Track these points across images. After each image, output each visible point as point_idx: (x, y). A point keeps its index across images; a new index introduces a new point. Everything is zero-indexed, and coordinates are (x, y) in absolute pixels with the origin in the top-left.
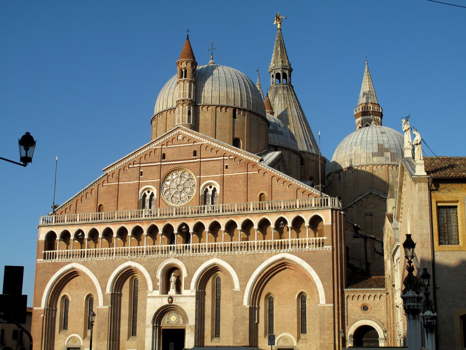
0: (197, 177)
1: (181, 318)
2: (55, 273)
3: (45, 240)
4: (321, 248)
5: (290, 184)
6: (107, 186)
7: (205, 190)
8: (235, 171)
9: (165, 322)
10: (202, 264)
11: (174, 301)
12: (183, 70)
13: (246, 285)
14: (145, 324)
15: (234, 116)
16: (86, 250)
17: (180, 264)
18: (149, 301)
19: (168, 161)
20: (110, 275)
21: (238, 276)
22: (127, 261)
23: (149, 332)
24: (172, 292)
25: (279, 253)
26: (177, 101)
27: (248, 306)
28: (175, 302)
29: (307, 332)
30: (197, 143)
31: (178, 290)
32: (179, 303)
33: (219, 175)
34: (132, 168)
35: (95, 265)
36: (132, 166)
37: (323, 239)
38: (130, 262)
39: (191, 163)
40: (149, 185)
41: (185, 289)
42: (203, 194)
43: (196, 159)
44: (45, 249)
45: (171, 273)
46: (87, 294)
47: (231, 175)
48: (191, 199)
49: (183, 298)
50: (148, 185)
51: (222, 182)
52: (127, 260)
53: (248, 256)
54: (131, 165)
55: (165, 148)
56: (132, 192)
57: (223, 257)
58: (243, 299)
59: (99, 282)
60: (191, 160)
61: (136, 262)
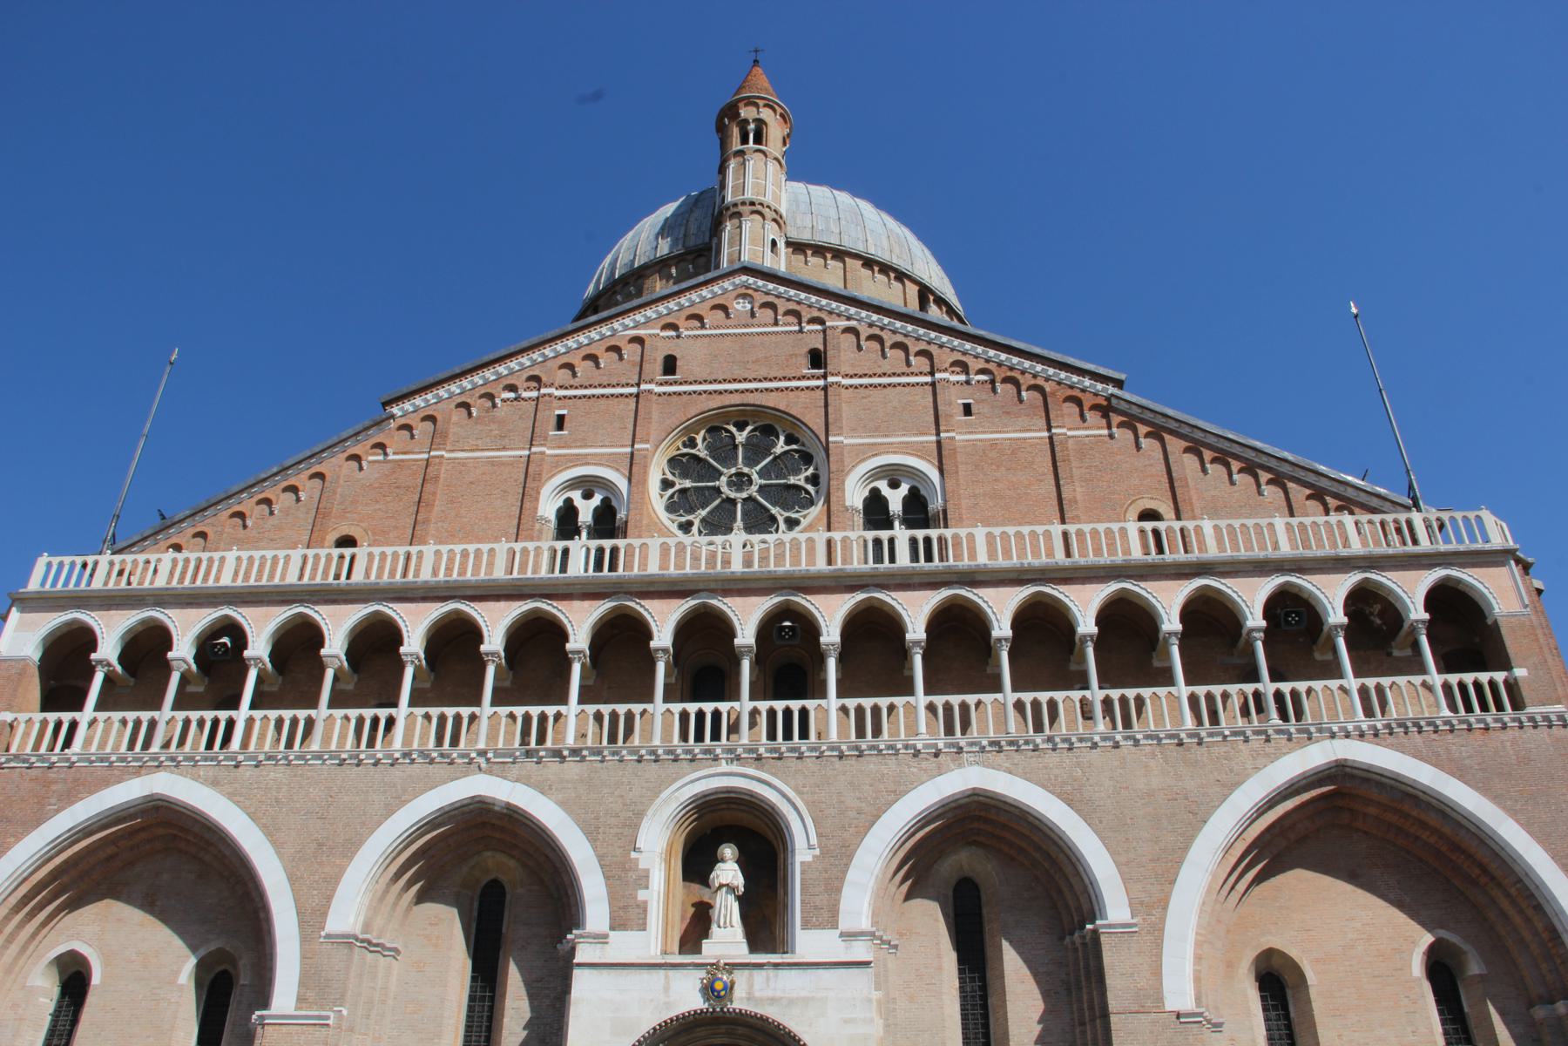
6: (389, 465)
7: (867, 494)
8: (1006, 425)
10: (898, 794)
11: (739, 992)
12: (752, 126)
13: (1164, 904)
18: (583, 985)
19: (691, 379)
20: (360, 843)
21: (1114, 854)
28: (748, 999)
30: (821, 322)
32: (773, 1000)
34: (515, 403)
35: (279, 790)
36: (512, 395)
37: (1512, 686)
39: (798, 393)
40: (595, 464)
42: (860, 506)
43: (825, 377)
46: (203, 952)
47: (994, 439)
49: (794, 973)
50: (587, 464)
53: (1154, 756)
54: (511, 391)
56: (505, 492)
57: (1017, 757)
58: (1157, 973)
60: (799, 379)
61: (517, 781)
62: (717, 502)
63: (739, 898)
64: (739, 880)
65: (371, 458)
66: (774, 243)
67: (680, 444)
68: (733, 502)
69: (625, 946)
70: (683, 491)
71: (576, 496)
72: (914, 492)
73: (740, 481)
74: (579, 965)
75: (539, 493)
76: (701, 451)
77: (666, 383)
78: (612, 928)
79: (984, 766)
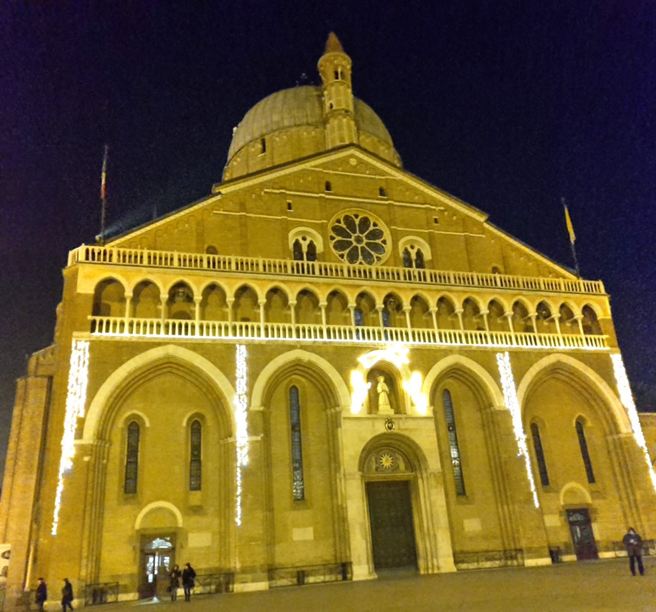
0: (392, 227)
9: (371, 466)
18: (346, 426)
28: (399, 429)
29: (596, 480)
30: (384, 176)
32: (406, 429)
38: (298, 351)
43: (387, 200)
52: (291, 347)
63: (389, 396)
64: (387, 389)
65: (215, 212)
70: (339, 241)
73: (359, 240)
74: (345, 418)
75: (288, 236)
76: (343, 225)
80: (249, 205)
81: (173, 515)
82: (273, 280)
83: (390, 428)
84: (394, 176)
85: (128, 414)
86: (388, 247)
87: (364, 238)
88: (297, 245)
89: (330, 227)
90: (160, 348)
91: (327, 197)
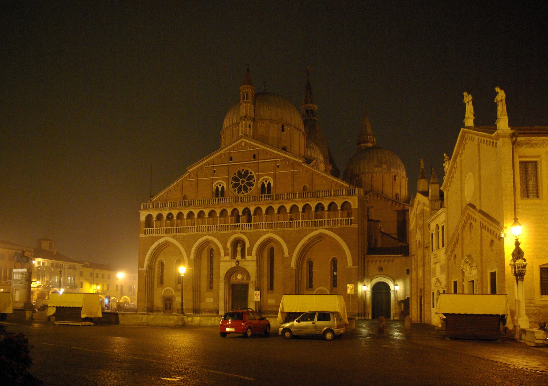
1: (245, 276)
2: (153, 244)
3: (145, 221)
4: (349, 226)
5: (326, 178)
7: (262, 183)
11: (240, 264)
14: (219, 281)
15: (283, 130)
16: (175, 227)
17: (244, 237)
18: (222, 264)
22: (205, 235)
23: (222, 285)
24: (239, 257)
25: (318, 229)
26: (241, 118)
27: (295, 268)
28: (241, 265)
29: (338, 286)
30: (256, 148)
31: (243, 256)
32: (244, 265)
33: (272, 173)
37: (351, 219)
40: (221, 180)
41: (248, 255)
42: (261, 186)
44: (146, 227)
45: (238, 244)
46: (176, 260)
48: (252, 190)
49: (246, 262)
51: (275, 177)
52: (205, 235)
53: (295, 231)
55: (232, 152)
59: (185, 250)
62: (239, 186)
65: (187, 180)
66: (250, 125)
67: (233, 174)
68: (242, 185)
69: (228, 258)
70: (234, 184)
71: (218, 185)
72: (269, 182)
73: (243, 182)
74: (221, 261)
75: (212, 186)
76: (237, 176)
77: (231, 163)
78: (225, 256)
79: (272, 233)
80: (199, 174)
81: (172, 291)
82: (200, 208)
83: (239, 264)
84: (260, 147)
85: (159, 260)
86: (255, 185)
87: (245, 180)
88: (217, 188)
89: (231, 177)
90: (163, 238)
91: (230, 164)
